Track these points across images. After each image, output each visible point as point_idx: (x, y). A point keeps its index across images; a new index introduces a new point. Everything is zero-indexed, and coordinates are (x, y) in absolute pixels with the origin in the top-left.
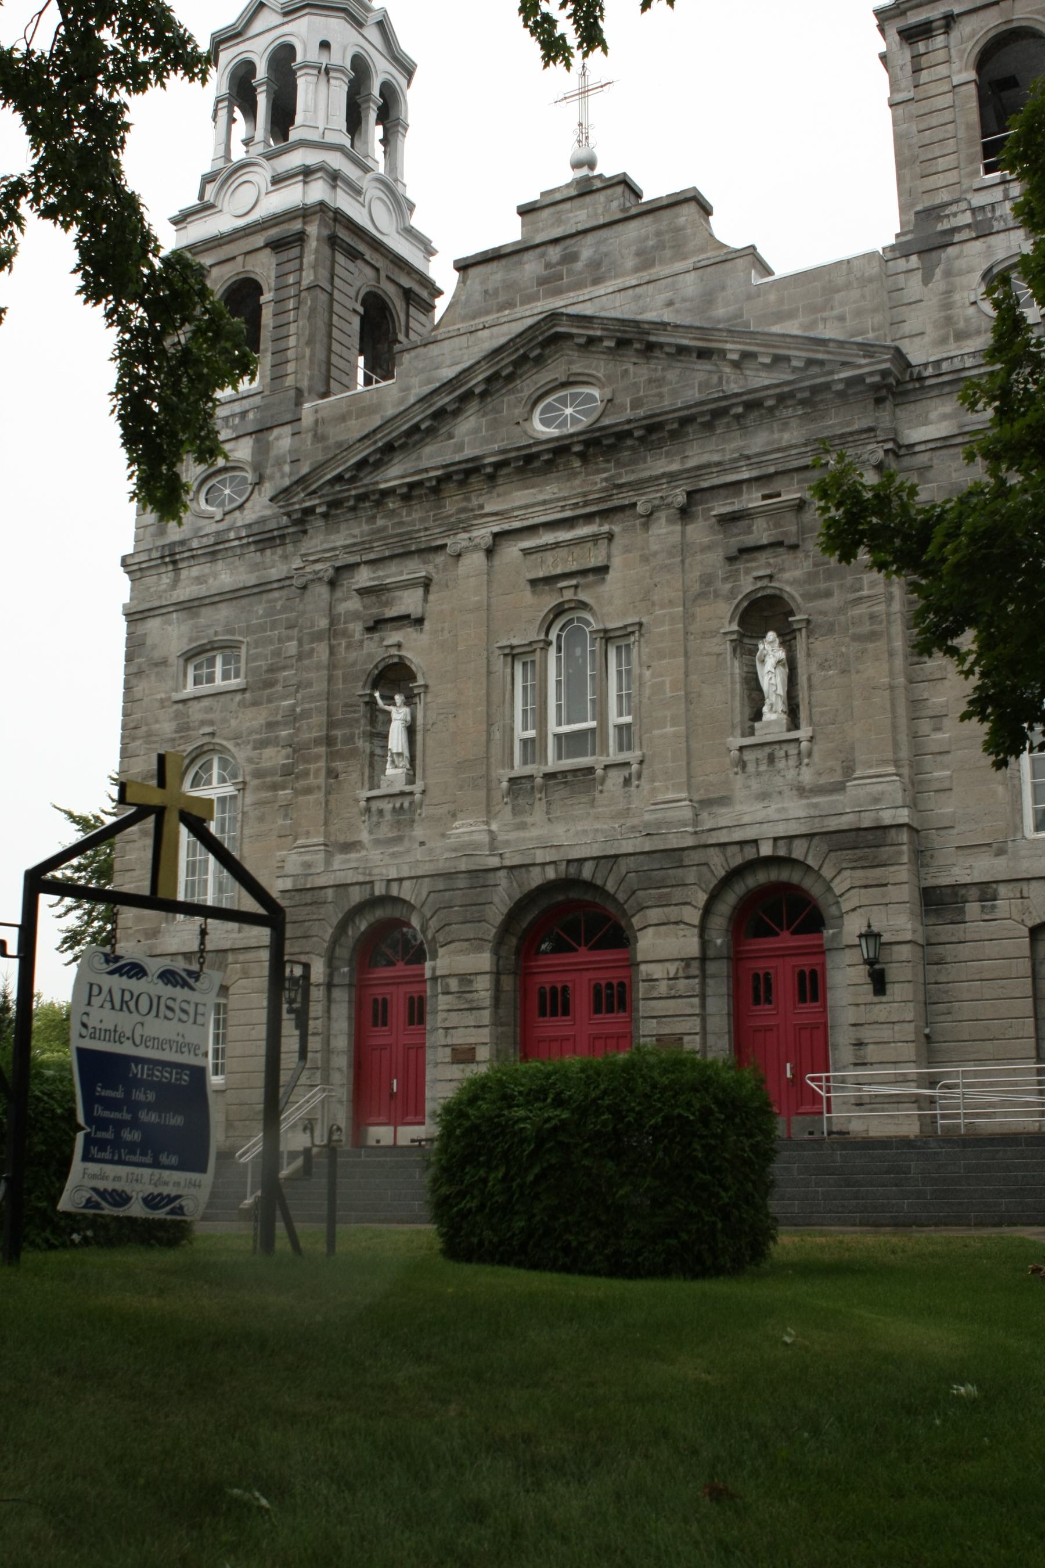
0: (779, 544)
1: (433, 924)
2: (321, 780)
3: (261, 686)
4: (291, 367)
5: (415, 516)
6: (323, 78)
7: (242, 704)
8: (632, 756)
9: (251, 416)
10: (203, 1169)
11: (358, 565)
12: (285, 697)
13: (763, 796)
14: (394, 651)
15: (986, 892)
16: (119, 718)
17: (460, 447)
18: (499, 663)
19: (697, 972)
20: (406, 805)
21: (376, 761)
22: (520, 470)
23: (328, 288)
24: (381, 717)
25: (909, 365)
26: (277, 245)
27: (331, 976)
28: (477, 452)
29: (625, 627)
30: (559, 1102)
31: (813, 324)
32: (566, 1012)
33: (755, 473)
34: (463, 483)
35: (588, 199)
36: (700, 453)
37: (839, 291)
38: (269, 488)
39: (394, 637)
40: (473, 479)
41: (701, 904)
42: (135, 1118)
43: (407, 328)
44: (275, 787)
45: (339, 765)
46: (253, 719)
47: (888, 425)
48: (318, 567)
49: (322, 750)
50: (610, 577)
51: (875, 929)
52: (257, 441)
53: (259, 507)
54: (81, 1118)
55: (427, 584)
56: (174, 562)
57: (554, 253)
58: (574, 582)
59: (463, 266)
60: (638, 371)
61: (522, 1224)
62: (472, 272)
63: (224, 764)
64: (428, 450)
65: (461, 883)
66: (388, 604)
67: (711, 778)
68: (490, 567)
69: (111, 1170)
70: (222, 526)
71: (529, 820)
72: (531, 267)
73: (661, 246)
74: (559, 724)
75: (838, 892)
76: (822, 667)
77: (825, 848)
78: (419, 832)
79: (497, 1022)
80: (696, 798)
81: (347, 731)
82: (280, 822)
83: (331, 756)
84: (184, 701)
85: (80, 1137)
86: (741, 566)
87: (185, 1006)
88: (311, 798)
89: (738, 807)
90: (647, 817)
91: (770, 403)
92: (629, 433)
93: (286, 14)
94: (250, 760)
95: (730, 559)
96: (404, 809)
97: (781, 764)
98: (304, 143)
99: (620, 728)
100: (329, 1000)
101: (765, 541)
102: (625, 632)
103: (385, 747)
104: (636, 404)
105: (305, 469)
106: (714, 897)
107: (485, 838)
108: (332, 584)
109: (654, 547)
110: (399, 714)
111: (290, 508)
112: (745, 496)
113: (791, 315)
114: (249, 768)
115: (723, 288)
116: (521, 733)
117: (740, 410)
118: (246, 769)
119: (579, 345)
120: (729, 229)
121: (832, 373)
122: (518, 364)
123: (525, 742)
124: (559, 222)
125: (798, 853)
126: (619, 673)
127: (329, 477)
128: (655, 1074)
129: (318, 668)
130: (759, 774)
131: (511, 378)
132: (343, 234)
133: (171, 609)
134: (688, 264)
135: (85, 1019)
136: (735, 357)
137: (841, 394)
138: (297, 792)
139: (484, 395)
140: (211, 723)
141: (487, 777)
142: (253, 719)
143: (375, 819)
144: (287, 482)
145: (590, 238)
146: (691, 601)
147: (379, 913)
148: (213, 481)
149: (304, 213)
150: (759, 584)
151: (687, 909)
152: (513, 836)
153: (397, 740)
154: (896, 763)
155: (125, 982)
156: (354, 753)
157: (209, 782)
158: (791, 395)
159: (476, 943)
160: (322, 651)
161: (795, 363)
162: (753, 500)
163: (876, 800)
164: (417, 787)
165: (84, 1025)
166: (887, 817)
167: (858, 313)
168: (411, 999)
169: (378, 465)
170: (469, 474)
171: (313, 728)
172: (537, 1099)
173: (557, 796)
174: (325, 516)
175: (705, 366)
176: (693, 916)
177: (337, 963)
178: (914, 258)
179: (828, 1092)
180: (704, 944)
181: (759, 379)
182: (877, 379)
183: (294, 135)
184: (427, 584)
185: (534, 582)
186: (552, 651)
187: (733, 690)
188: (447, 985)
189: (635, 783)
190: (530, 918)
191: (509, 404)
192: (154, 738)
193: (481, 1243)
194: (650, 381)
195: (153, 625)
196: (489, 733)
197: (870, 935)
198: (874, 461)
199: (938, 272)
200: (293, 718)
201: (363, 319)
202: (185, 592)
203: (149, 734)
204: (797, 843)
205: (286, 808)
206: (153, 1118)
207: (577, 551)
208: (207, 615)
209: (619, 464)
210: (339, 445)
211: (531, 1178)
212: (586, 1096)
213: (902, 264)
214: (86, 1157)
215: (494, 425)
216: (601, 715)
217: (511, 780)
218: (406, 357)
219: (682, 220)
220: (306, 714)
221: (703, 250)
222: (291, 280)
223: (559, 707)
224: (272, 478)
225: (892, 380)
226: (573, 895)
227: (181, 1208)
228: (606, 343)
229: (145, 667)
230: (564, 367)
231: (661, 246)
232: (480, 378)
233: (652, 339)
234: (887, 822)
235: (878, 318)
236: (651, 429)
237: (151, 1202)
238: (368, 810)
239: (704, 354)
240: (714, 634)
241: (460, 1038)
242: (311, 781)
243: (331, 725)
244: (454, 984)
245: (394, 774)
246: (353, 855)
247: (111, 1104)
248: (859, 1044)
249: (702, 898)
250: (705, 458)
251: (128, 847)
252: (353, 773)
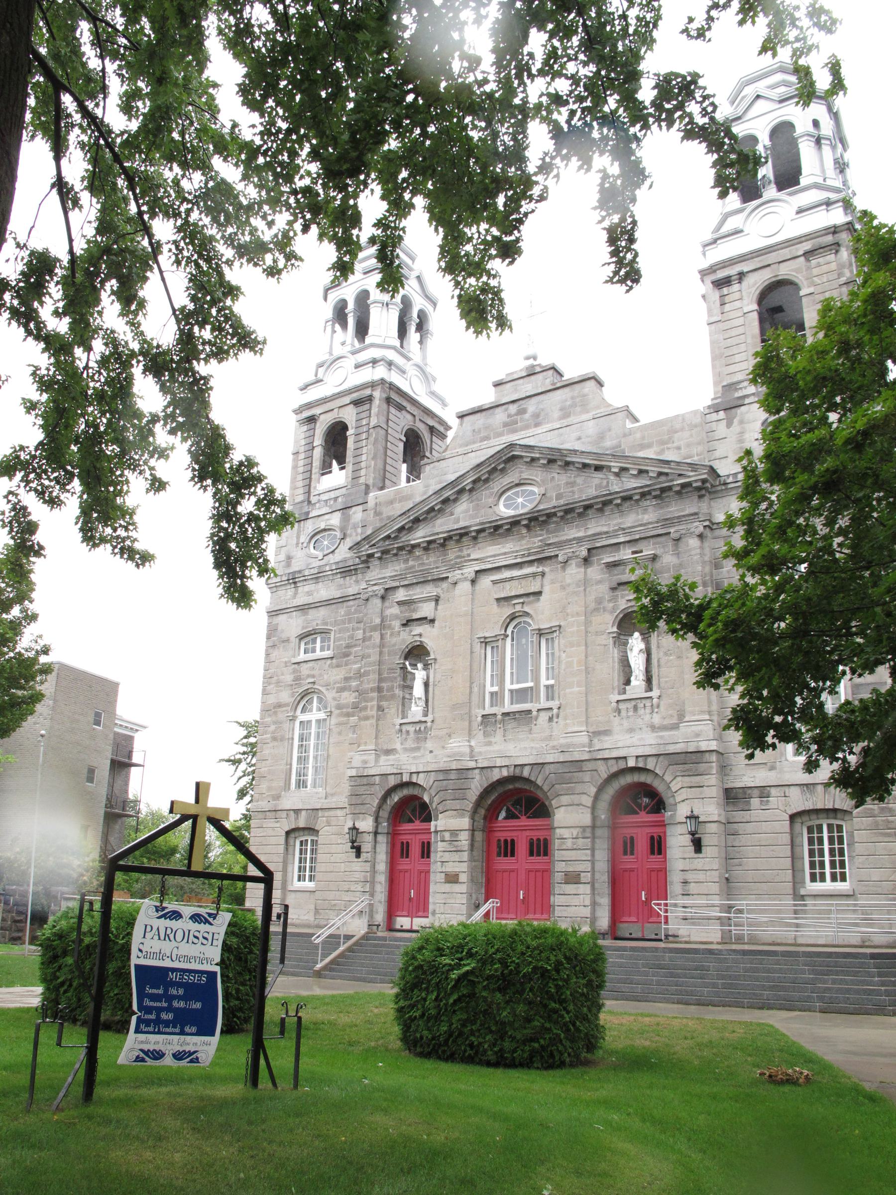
1: (436, 800)
2: (374, 713)
3: (343, 655)
4: (363, 472)
5: (431, 559)
6: (385, 308)
7: (331, 666)
8: (554, 704)
9: (340, 500)
10: (212, 1034)
11: (398, 587)
12: (355, 663)
13: (631, 730)
14: (417, 638)
15: (764, 792)
16: (261, 672)
17: (457, 520)
18: (477, 647)
19: (589, 835)
21: (405, 703)
23: (385, 427)
24: (409, 676)
25: (719, 476)
26: (357, 403)
27: (377, 827)
28: (466, 524)
30: (470, 955)
31: (662, 452)
32: (513, 855)
33: (628, 539)
34: (458, 541)
35: (532, 377)
36: (595, 526)
37: (676, 432)
38: (349, 542)
39: (417, 629)
40: (464, 539)
41: (593, 794)
42: (170, 1005)
43: (431, 449)
44: (348, 715)
45: (384, 704)
46: (336, 675)
47: (706, 511)
48: (375, 588)
49: (375, 694)
50: (543, 598)
51: (696, 813)
52: (343, 514)
53: (343, 553)
54: (135, 1007)
55: (437, 600)
56: (295, 583)
57: (513, 408)
58: (521, 600)
59: (461, 416)
60: (560, 478)
61: (445, 1028)
62: (466, 419)
63: (320, 700)
64: (439, 522)
66: (414, 610)
67: (600, 718)
68: (473, 591)
69: (152, 1037)
70: (322, 563)
71: (493, 740)
72: (500, 416)
73: (574, 405)
74: (512, 683)
75: (674, 790)
76: (666, 654)
77: (666, 763)
78: (429, 745)
79: (472, 859)
80: (591, 730)
81: (389, 684)
82: (351, 735)
83: (381, 698)
85: (134, 1019)
86: (618, 593)
87: (206, 935)
88: (368, 722)
89: (616, 737)
90: (562, 741)
91: (637, 497)
92: (555, 514)
93: (365, 273)
94: (334, 699)
95: (613, 589)
96: (422, 730)
97: (641, 712)
98: (372, 345)
99: (547, 687)
100: (376, 842)
102: (551, 631)
103: (411, 694)
104: (559, 496)
105: (369, 532)
106: (601, 789)
107: (468, 750)
108: (383, 598)
109: (568, 581)
110: (420, 675)
112: (622, 552)
113: (649, 446)
114: (334, 703)
115: (610, 430)
116: (489, 689)
117: (619, 501)
118: (332, 704)
120: (614, 395)
121: (672, 480)
122: (491, 472)
123: (492, 694)
124: (516, 390)
125: (650, 766)
126: (547, 654)
128: (529, 939)
129: (374, 647)
130: (628, 717)
131: (487, 481)
132: (394, 396)
134: (589, 416)
135: (141, 947)
136: (616, 470)
137: (679, 493)
138: (360, 719)
139: (471, 490)
140: (313, 676)
141: (469, 714)
142: (336, 675)
144: (359, 538)
145: (534, 400)
146: (588, 614)
147: (406, 792)
148: (318, 537)
149: (372, 385)
150: (630, 604)
151: (584, 796)
152: (484, 749)
153: (418, 690)
154: (710, 713)
155: (168, 923)
156: (393, 697)
157: (311, 710)
158: (649, 493)
159: (460, 812)
160: (376, 636)
161: (651, 474)
162: (626, 554)
163: (698, 735)
164: (429, 719)
165: (140, 950)
166: (704, 746)
167: (688, 445)
169: (410, 530)
170: (461, 535)
171: (370, 682)
172: (457, 952)
173: (509, 726)
174: (380, 558)
175: (599, 475)
176: (588, 801)
177: (380, 820)
178: (722, 413)
179: (666, 911)
180: (594, 818)
181: (631, 483)
182: (699, 484)
183: (368, 340)
184: (437, 600)
185: (498, 600)
186: (509, 640)
187: (613, 667)
189: (555, 720)
190: (493, 798)
191: (485, 495)
193: (422, 1038)
194: (567, 483)
195: (282, 618)
196: (471, 688)
197: (693, 817)
198: (697, 533)
199: (736, 421)
200: (359, 675)
201: (406, 444)
202: (301, 600)
203: (278, 682)
204: (650, 759)
205: (354, 727)
206: (182, 1004)
207: (523, 582)
208: (313, 614)
209: (548, 532)
210: (389, 517)
211: (451, 1001)
212: (486, 952)
213: (714, 416)
214: (137, 1031)
215: (477, 508)
216: (537, 680)
218: (428, 468)
219: (586, 390)
220: (367, 673)
221: (598, 407)
222: (364, 422)
223: (512, 673)
224: (351, 536)
225: (708, 485)
226: (518, 785)
227: (197, 1058)
228: (542, 461)
230: (517, 475)
231: (574, 405)
233: (568, 459)
234: (704, 749)
235: (700, 448)
236: (567, 512)
237: (178, 1056)
238: (401, 731)
239: (598, 468)
240: (602, 633)
241: (450, 868)
242: (369, 712)
243: (381, 680)
244: (447, 836)
245: (416, 711)
246: (391, 757)
247: (154, 997)
248: (685, 882)
249: (593, 790)
250: (599, 529)
252: (392, 709)
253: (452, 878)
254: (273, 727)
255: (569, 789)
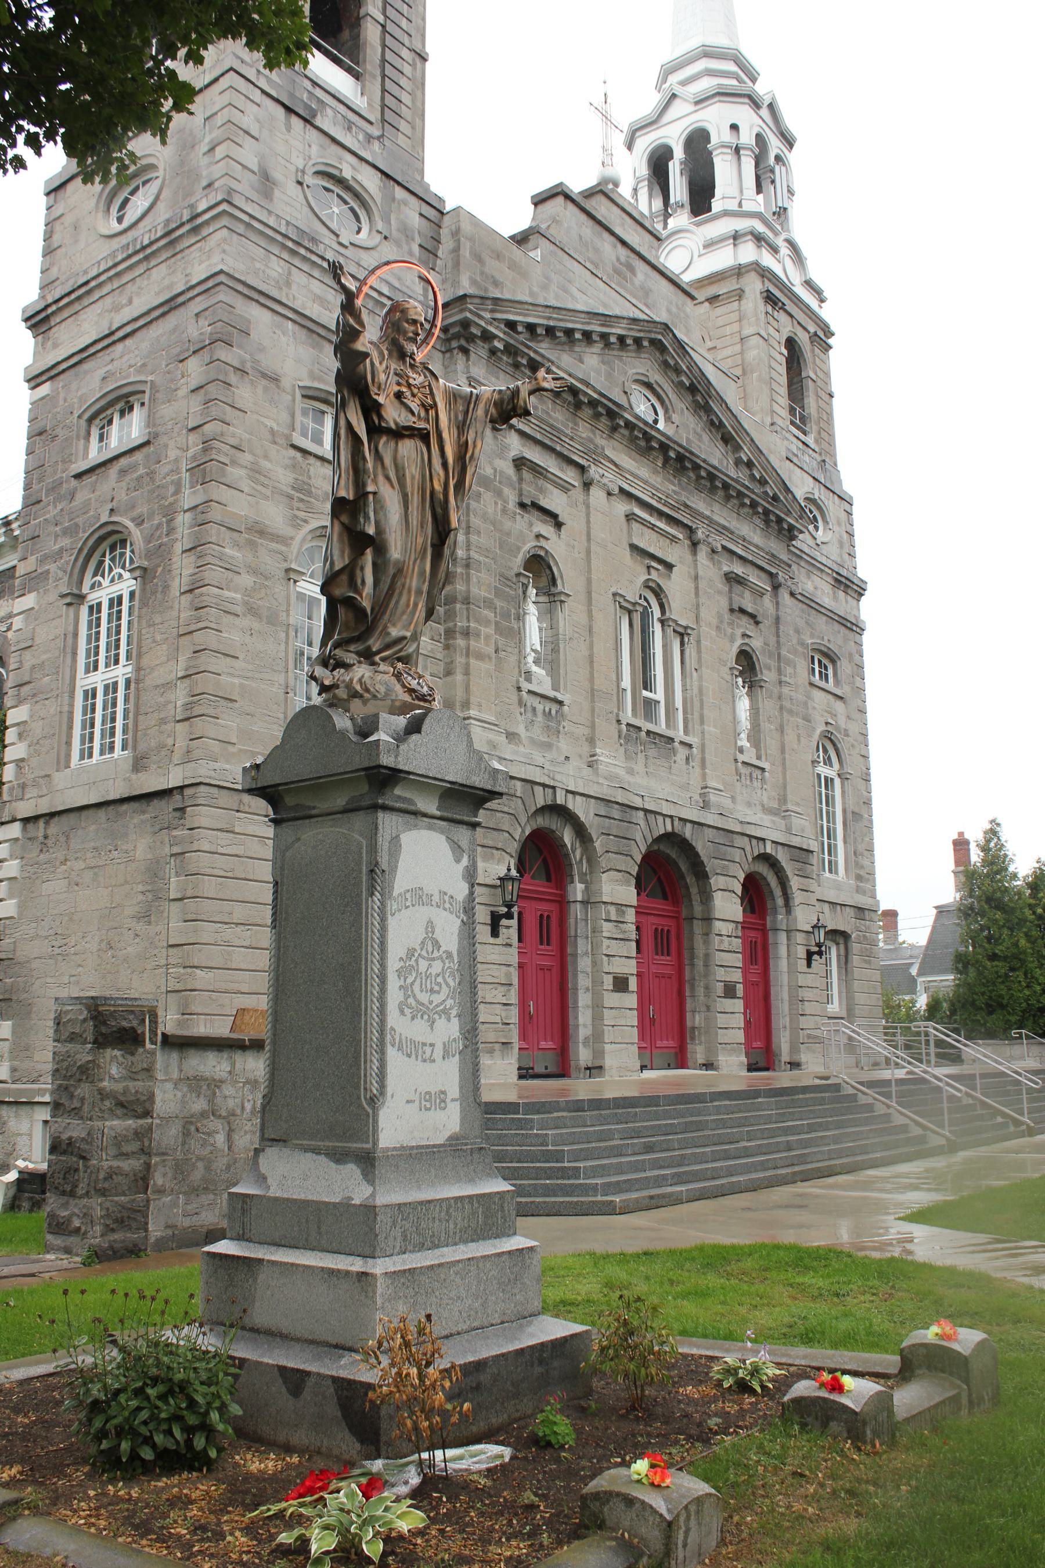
0: (753, 616)
2: (491, 650)
20: (553, 712)
22: (633, 440)
29: (686, 628)
34: (597, 416)
65: (616, 813)
78: (564, 745)
84: (305, 452)
91: (760, 510)
92: (696, 467)
101: (750, 610)
111: (476, 320)
119: (666, 363)
127: (511, 317)
133: (290, 315)
143: (529, 715)
168: (541, 916)
174: (493, 352)
185: (634, 548)
188: (608, 913)
192: (262, 478)
203: (255, 471)
207: (662, 539)
217: (628, 725)
229: (248, 367)
232: (620, 332)
239: (727, 439)
251: (227, 619)
253: (620, 984)
254: (246, 580)
255: (724, 867)
